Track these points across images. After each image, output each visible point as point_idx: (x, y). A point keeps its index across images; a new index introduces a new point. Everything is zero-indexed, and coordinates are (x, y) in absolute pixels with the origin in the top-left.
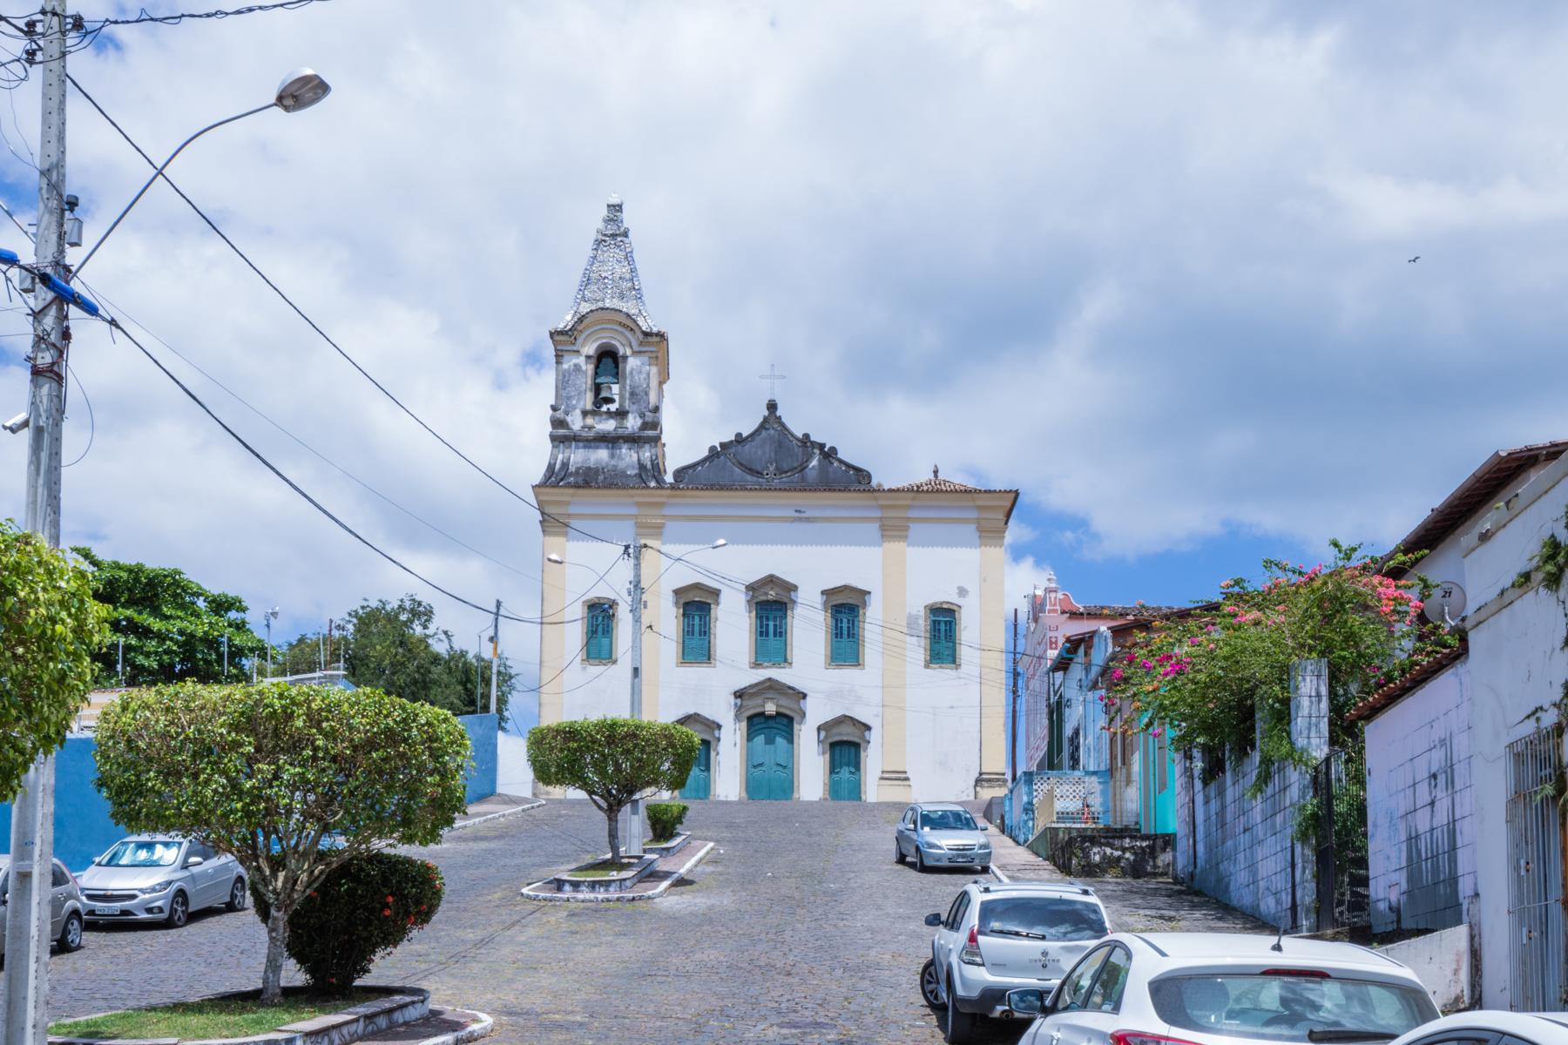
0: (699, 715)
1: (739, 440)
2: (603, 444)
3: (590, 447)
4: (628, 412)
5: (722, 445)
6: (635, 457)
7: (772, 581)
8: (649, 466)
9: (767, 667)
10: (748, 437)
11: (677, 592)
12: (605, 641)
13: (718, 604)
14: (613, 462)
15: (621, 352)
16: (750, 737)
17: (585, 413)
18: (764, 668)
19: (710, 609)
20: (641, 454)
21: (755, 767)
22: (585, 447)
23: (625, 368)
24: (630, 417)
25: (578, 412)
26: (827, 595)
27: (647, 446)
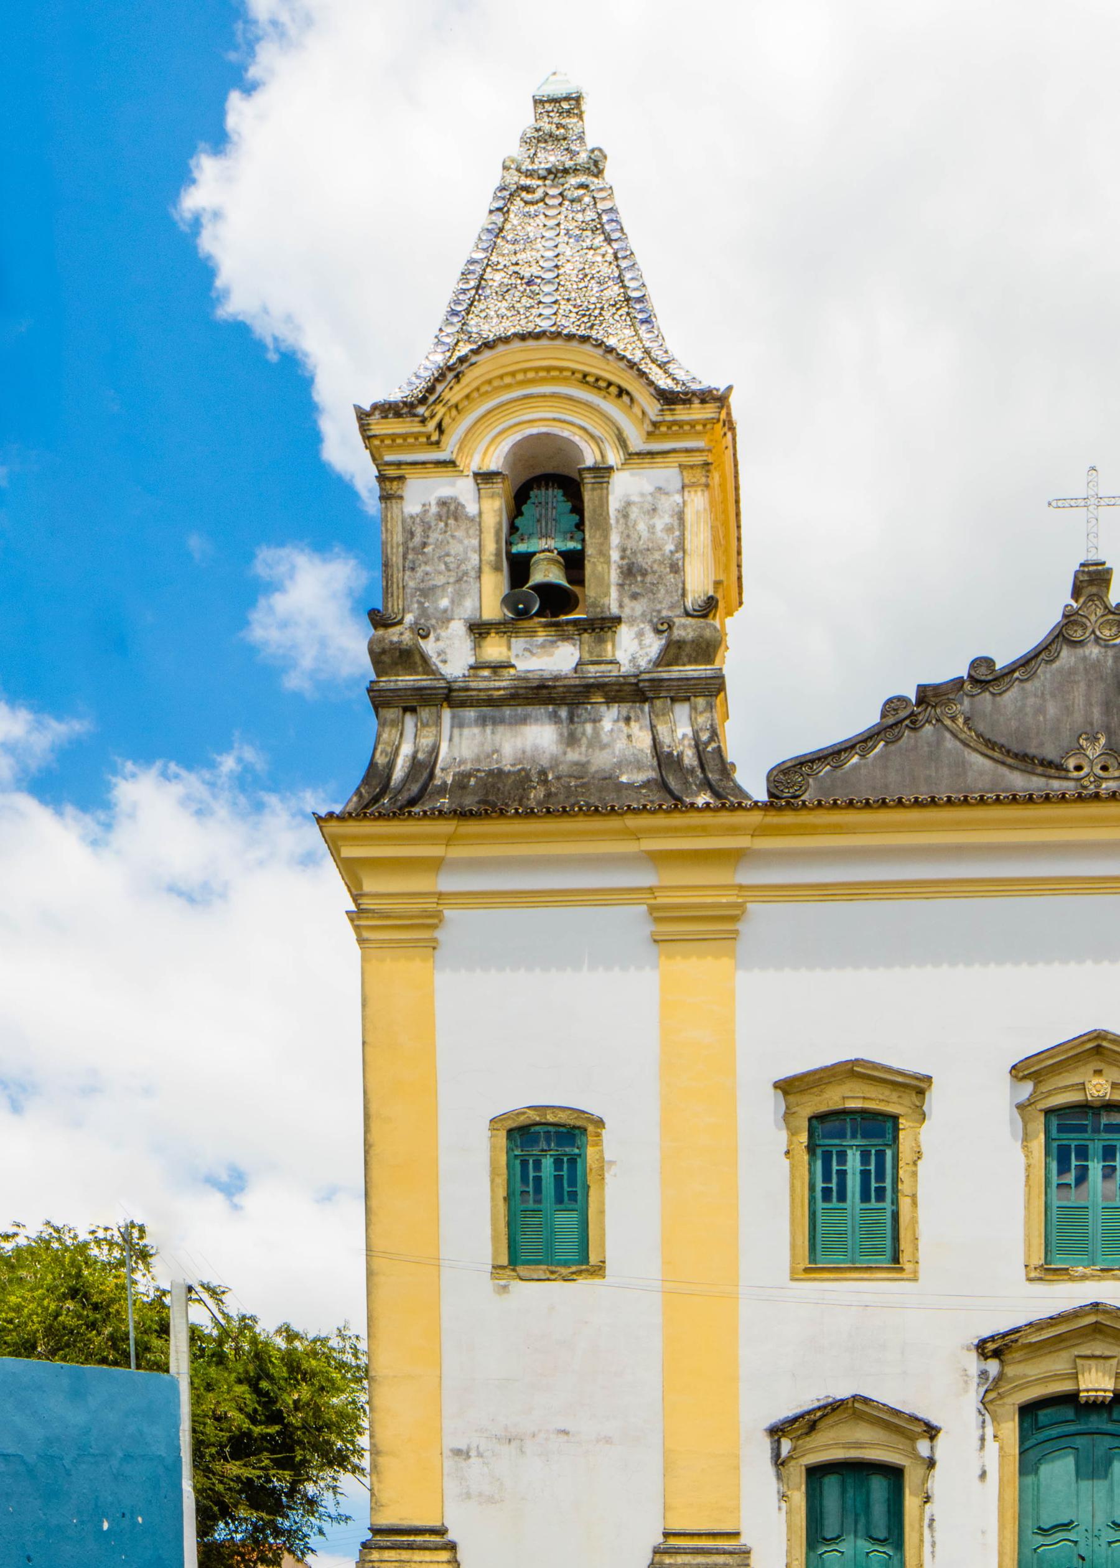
0: (866, 1400)
2: (541, 711)
3: (497, 722)
4: (618, 620)
6: (643, 740)
7: (1098, 1050)
8: (689, 758)
10: (1011, 670)
11: (787, 1087)
12: (565, 1220)
13: (922, 1116)
14: (573, 755)
15: (590, 458)
16: (1028, 1463)
17: (479, 630)
20: (662, 729)
21: (1043, 1531)
22: (482, 721)
23: (603, 503)
24: (625, 634)
25: (458, 628)
27: (682, 711)
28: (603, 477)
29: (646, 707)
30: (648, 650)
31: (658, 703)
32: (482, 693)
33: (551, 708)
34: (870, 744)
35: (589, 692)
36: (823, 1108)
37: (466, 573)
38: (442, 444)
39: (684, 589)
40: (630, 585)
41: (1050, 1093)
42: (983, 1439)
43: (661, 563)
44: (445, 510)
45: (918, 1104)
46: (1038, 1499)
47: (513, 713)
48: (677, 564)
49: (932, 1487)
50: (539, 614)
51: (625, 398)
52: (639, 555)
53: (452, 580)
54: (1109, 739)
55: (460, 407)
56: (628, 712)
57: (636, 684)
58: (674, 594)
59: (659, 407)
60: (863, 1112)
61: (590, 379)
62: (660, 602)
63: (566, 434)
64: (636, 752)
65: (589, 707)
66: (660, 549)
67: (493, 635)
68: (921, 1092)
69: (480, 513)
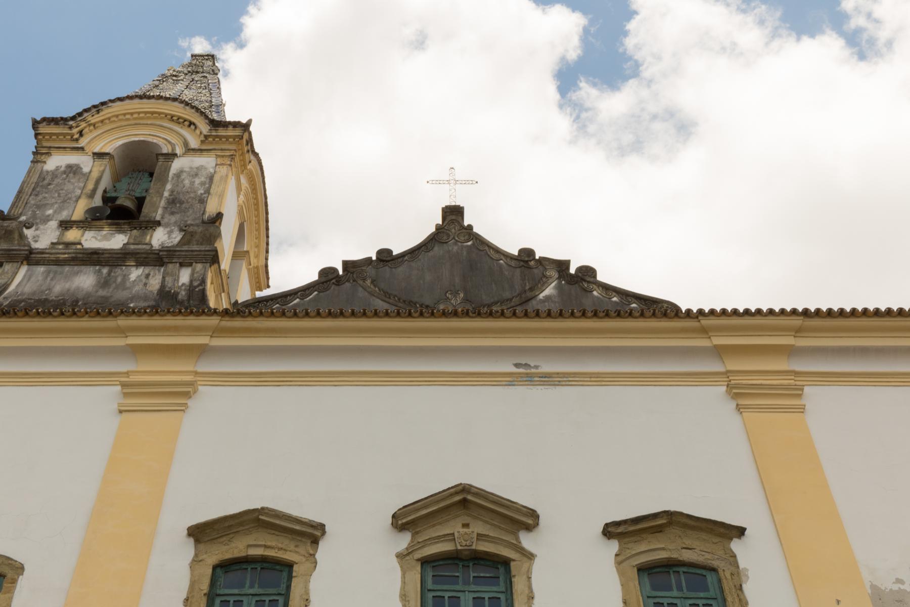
1: (385, 256)
4: (159, 224)
5: (346, 264)
10: (402, 255)
14: (102, 293)
19: (290, 577)
23: (168, 169)
26: (619, 536)
28: (170, 159)
29: (162, 269)
30: (173, 240)
31: (170, 266)
32: (53, 256)
33: (97, 268)
34: (307, 292)
35: (126, 258)
36: (228, 556)
37: (70, 199)
38: (79, 141)
39: (204, 211)
40: (171, 208)
41: (425, 543)
43: (193, 198)
44: (69, 169)
45: (311, 552)
47: (71, 269)
48: (204, 200)
50: (108, 218)
51: (193, 127)
52: (181, 194)
53: (59, 201)
54: (465, 294)
55: (96, 126)
56: (150, 271)
57: (158, 254)
58: (198, 213)
59: (209, 128)
60: (263, 560)
61: (175, 118)
62: (188, 217)
63: (155, 141)
64: (147, 292)
65: (124, 268)
66: (195, 192)
67: (74, 228)
68: (315, 541)
69: (91, 172)
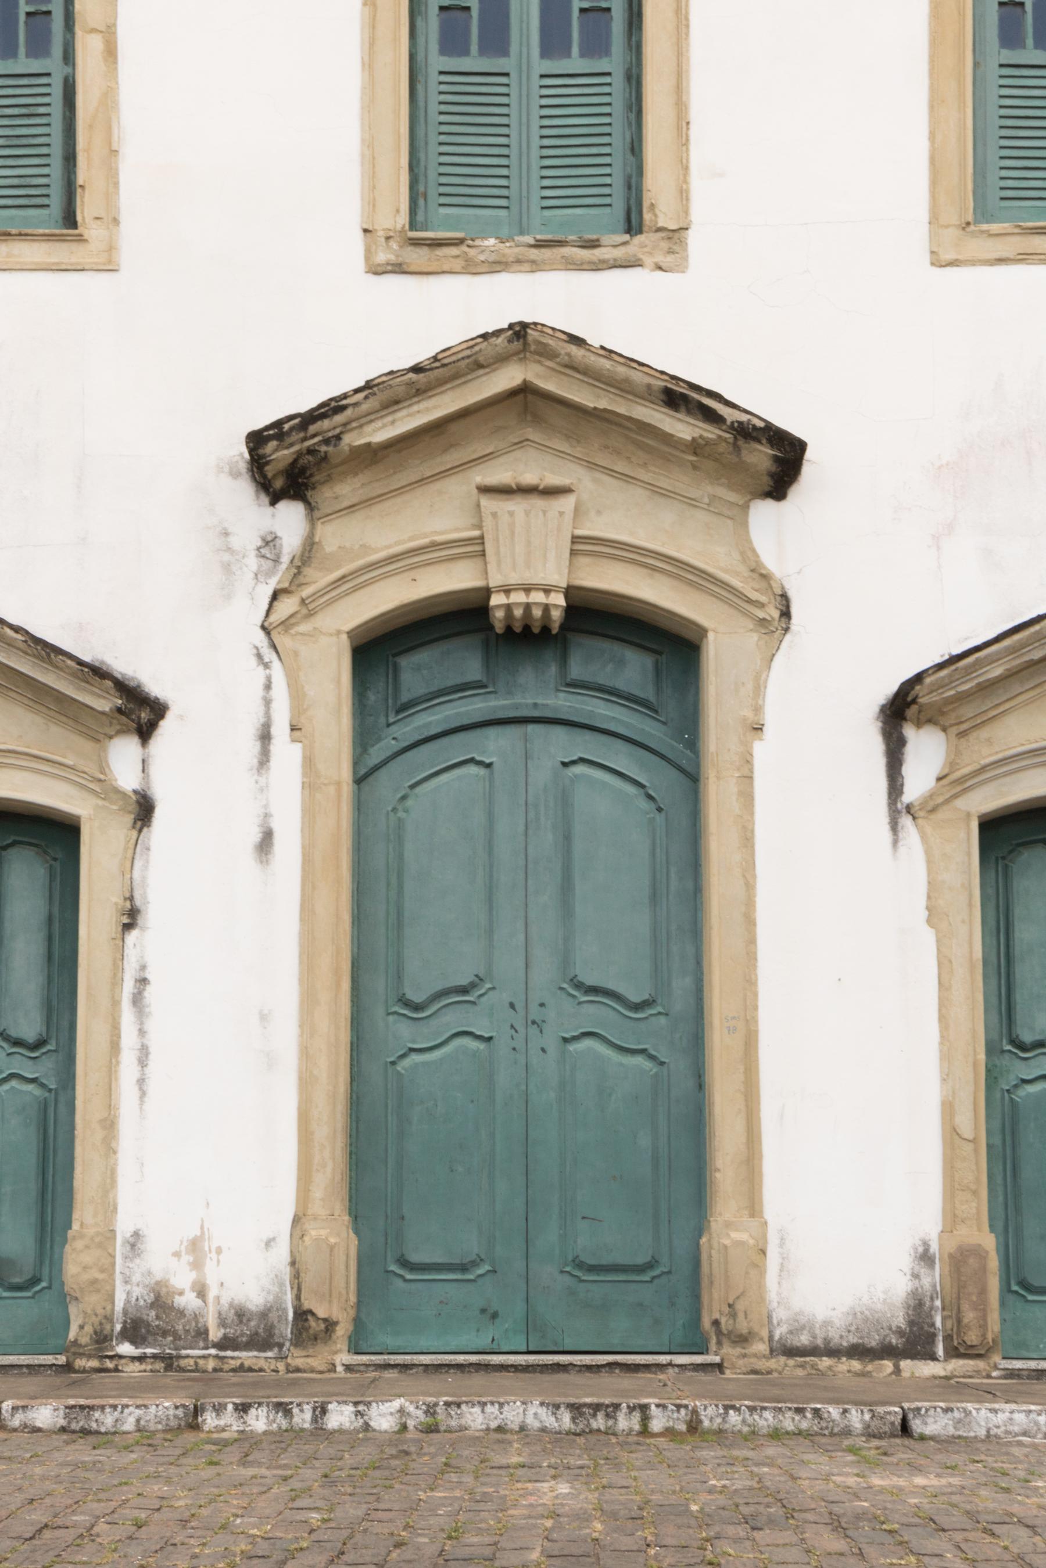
9: (498, 266)
18: (471, 268)
42: (265, 736)
46: (400, 914)
49: (144, 878)
